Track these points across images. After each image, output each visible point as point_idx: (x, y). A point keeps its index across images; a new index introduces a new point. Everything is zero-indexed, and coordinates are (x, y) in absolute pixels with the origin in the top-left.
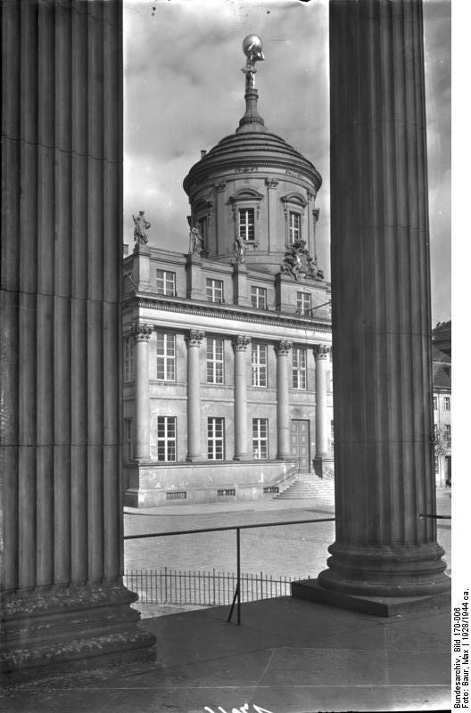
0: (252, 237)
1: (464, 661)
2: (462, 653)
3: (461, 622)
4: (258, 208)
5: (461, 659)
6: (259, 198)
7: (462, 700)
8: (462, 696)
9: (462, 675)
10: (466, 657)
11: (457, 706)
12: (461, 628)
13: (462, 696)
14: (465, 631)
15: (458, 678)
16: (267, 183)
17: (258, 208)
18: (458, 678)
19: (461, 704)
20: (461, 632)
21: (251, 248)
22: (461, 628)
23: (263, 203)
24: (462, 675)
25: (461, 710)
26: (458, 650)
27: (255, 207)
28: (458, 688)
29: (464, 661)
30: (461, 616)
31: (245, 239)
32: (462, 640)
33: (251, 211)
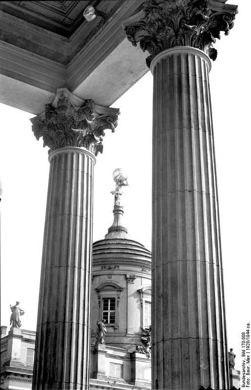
0: (112, 321)
1: (247, 361)
2: (246, 357)
3: (245, 340)
4: (119, 298)
5: (245, 360)
6: (120, 290)
7: (246, 383)
8: (246, 381)
9: (246, 369)
10: (248, 359)
11: (243, 386)
12: (245, 344)
13: (246, 381)
14: (248, 345)
15: (244, 371)
16: (126, 278)
17: (119, 298)
18: (244, 371)
19: (245, 385)
20: (246, 346)
21: (111, 330)
22: (245, 344)
23: (122, 294)
24: (246, 369)
25: (246, 388)
26: (243, 355)
27: (116, 297)
28: (244, 376)
29: (247, 361)
30: (246, 337)
31: (107, 322)
32: (246, 351)
33: (113, 300)
